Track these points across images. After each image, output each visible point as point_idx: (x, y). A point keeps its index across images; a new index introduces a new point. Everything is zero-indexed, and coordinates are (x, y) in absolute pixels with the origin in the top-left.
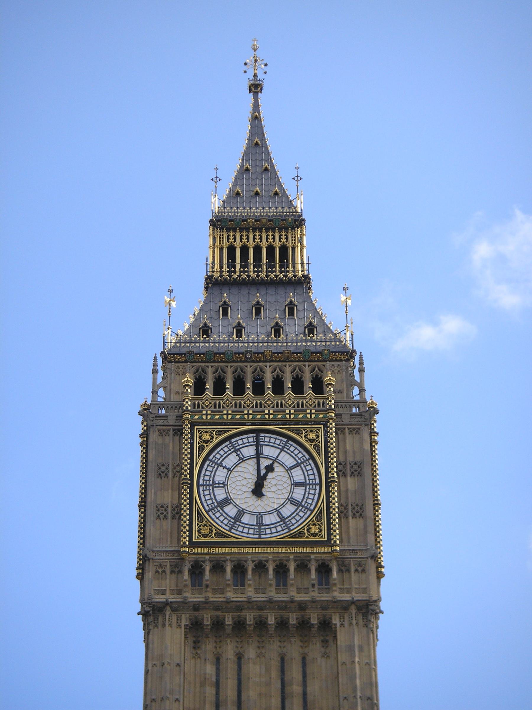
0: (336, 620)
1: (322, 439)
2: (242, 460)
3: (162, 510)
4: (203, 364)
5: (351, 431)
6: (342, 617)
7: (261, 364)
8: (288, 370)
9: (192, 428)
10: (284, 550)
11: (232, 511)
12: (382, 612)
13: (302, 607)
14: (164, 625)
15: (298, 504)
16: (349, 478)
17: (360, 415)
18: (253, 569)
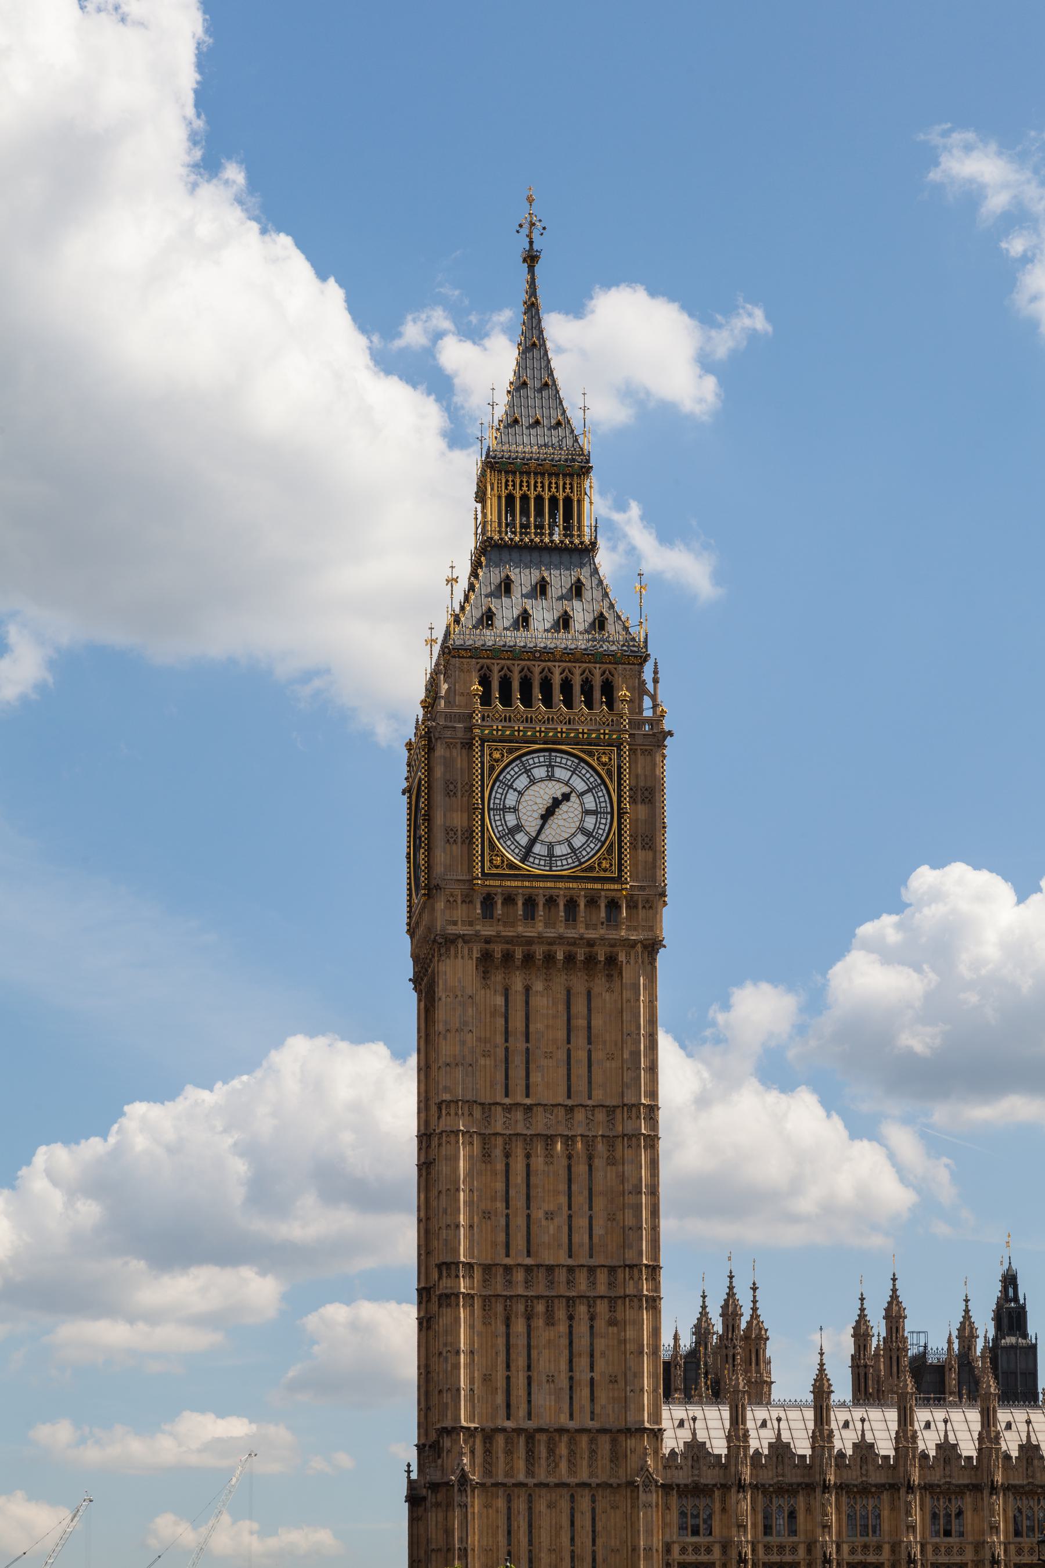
0: (622, 957)
1: (615, 762)
2: (533, 782)
3: (451, 834)
5: (643, 752)
6: (628, 955)
7: (549, 664)
8: (578, 672)
9: (482, 745)
10: (575, 885)
12: (665, 946)
13: (591, 943)
14: (456, 957)
15: (588, 834)
16: (639, 806)
17: (654, 735)
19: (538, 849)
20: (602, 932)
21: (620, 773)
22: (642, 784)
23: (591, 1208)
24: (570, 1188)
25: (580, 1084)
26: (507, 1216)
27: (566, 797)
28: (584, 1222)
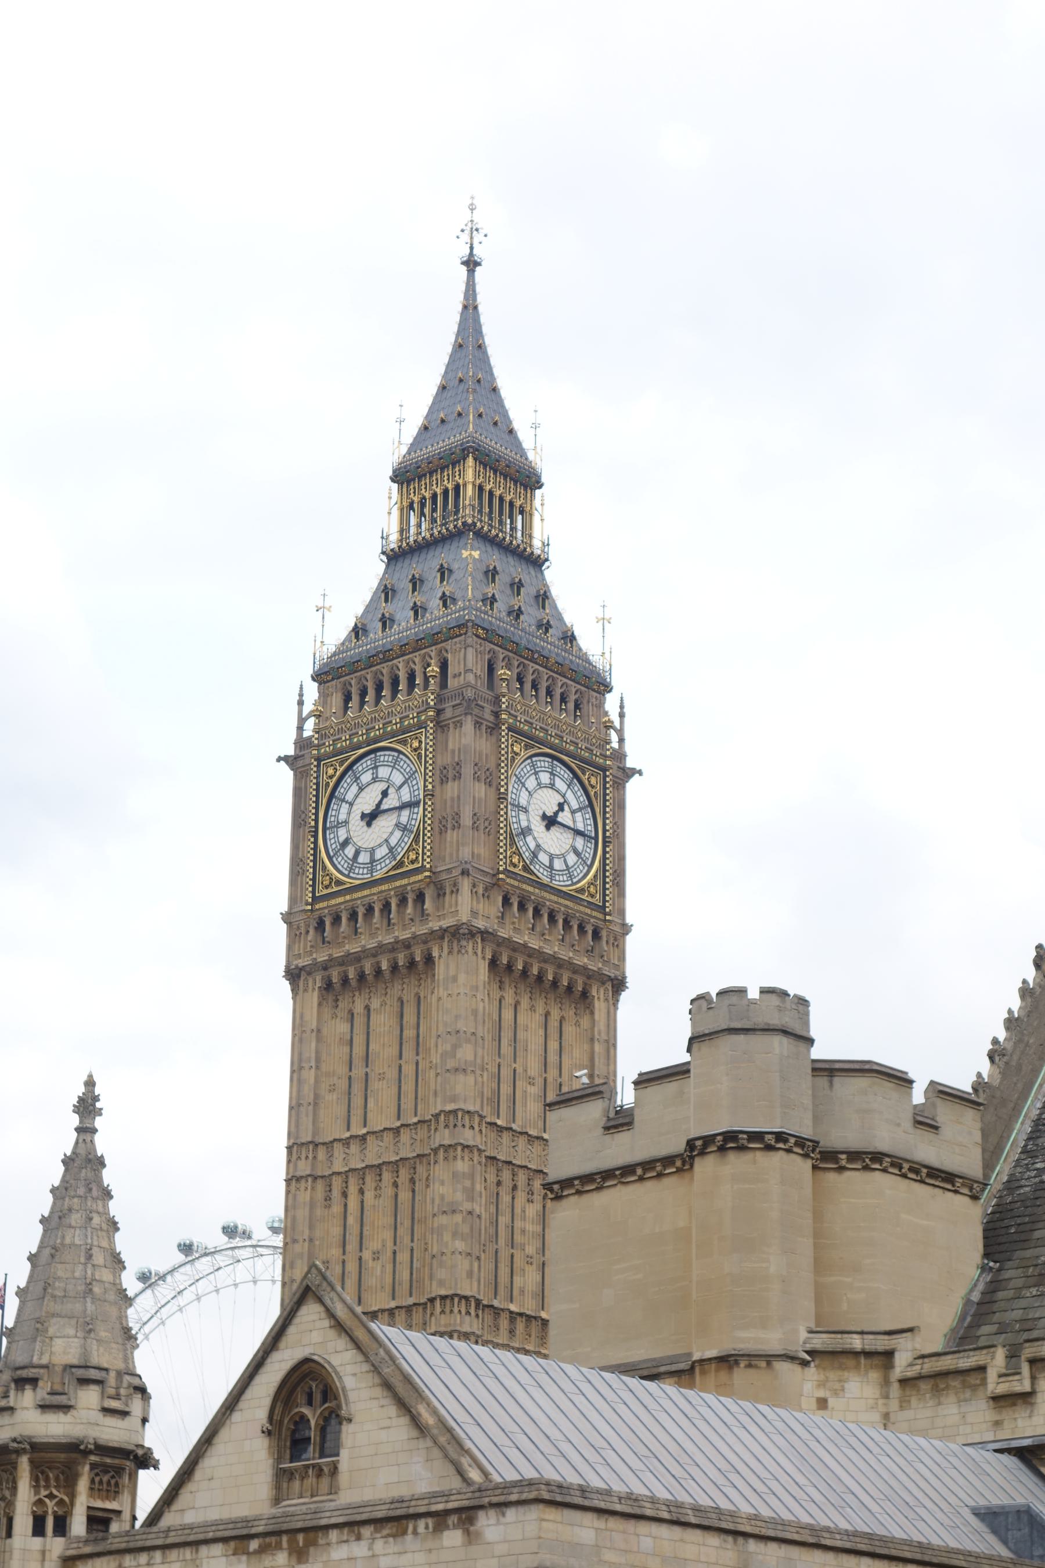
2: (361, 789)
4: (347, 678)
7: (395, 661)
9: (318, 766)
11: (350, 851)
13: (407, 945)
15: (404, 829)
16: (450, 783)
18: (365, 915)
19: (361, 859)
20: (413, 929)
21: (426, 756)
22: (456, 759)
23: (412, 1241)
24: (396, 1220)
25: (408, 1103)
26: (344, 1262)
27: (385, 794)
28: (403, 1257)
